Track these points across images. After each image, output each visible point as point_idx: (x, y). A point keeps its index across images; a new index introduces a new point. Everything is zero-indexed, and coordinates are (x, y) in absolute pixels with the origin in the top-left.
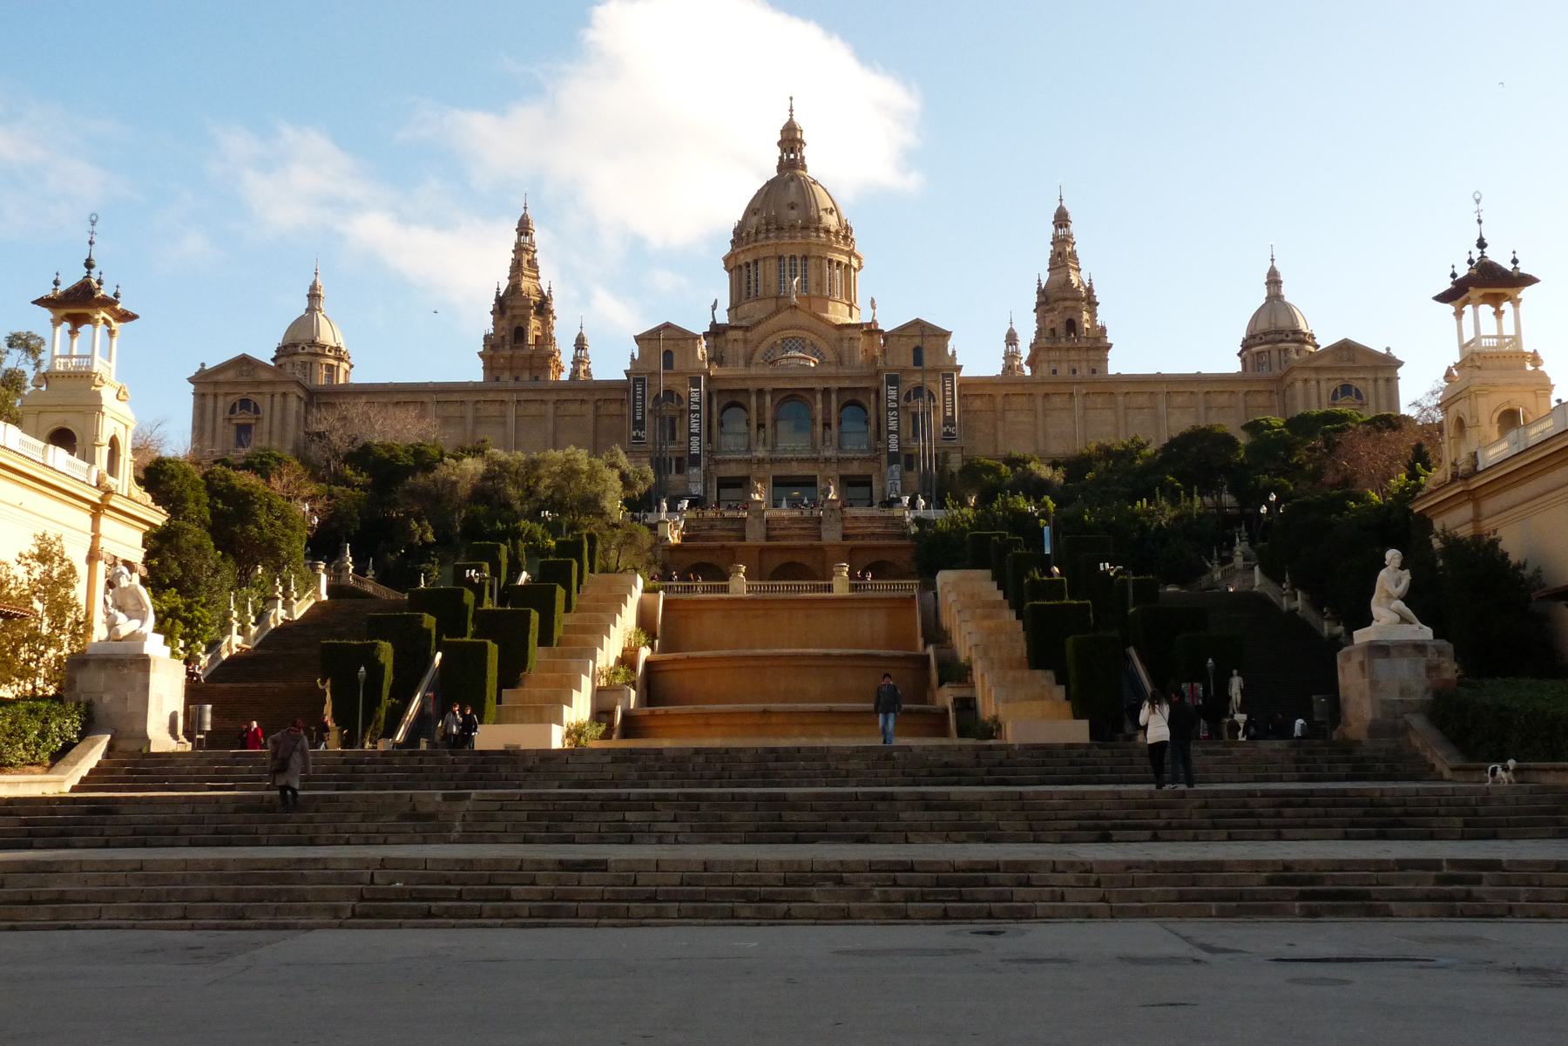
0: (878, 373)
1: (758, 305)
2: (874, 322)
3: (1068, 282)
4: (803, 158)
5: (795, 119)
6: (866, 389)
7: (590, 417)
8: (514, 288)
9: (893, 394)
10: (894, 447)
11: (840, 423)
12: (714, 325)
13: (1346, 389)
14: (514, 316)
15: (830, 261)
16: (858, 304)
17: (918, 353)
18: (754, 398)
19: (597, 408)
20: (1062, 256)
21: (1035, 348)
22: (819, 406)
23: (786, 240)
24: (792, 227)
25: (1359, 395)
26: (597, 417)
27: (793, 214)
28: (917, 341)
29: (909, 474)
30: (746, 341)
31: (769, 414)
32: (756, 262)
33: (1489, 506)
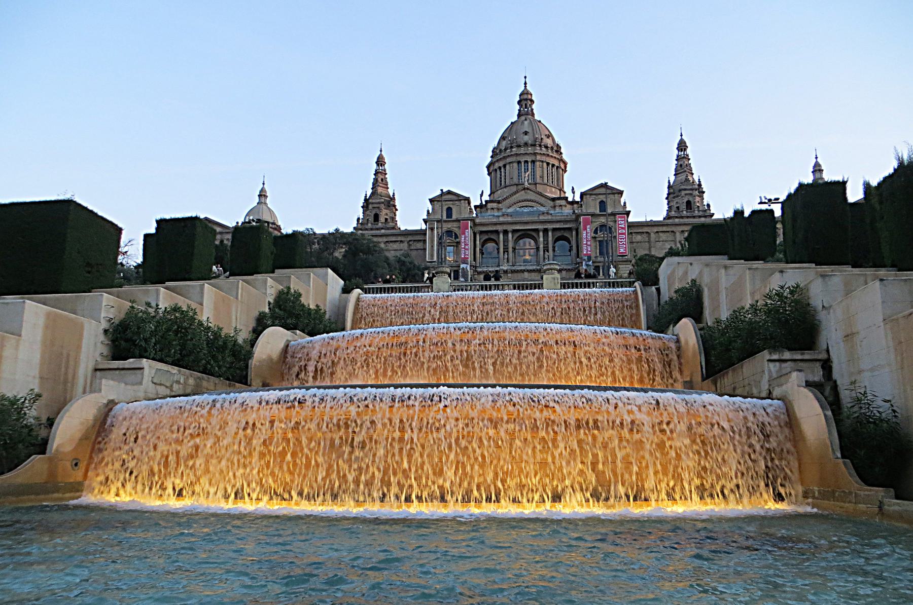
0: (578, 216)
1: (505, 190)
3: (687, 180)
6: (570, 229)
11: (554, 250)
15: (548, 164)
16: (565, 189)
17: (603, 205)
18: (501, 236)
19: (410, 245)
20: (683, 166)
21: (668, 217)
22: (541, 239)
24: (526, 144)
27: (526, 138)
28: (602, 198)
31: (511, 245)
32: (505, 166)
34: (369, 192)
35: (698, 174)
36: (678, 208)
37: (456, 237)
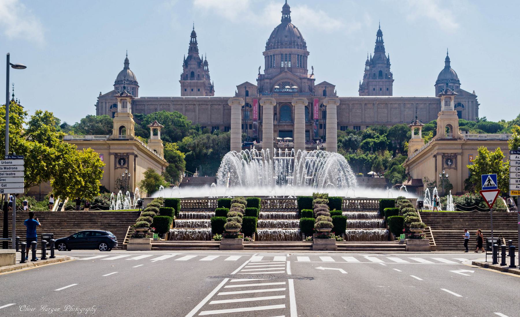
1: (274, 70)
3: (380, 57)
4: (290, 17)
5: (288, 3)
7: (222, 109)
8: (190, 57)
12: (259, 74)
14: (191, 68)
15: (298, 55)
19: (224, 107)
20: (380, 47)
24: (286, 44)
25: (463, 106)
26: (224, 110)
27: (286, 39)
28: (324, 88)
29: (321, 130)
30: (270, 83)
31: (278, 110)
32: (274, 55)
33: (411, 167)
34: (187, 56)
35: (388, 52)
36: (375, 74)
37: (251, 107)
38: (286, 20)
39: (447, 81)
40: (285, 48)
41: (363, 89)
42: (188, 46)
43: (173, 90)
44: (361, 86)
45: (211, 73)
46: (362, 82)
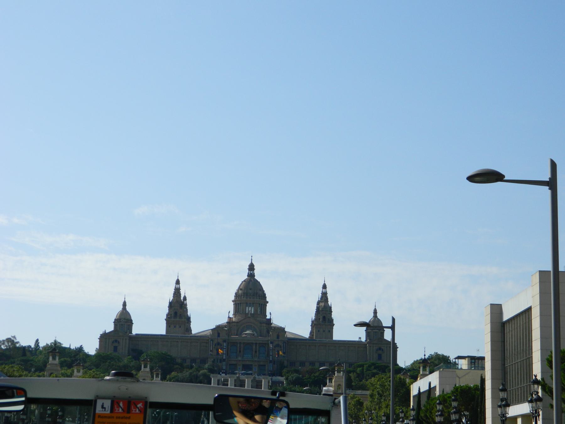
2: (270, 319)
9: (271, 346)
10: (271, 359)
11: (259, 351)
12: (229, 317)
13: (380, 349)
17: (278, 337)
20: (324, 297)
23: (248, 299)
25: (383, 350)
27: (250, 291)
34: (172, 298)
38: (251, 275)
39: (374, 328)
40: (250, 298)
41: (314, 324)
42: (173, 291)
43: (160, 329)
44: (312, 322)
45: (189, 307)
46: (314, 318)
